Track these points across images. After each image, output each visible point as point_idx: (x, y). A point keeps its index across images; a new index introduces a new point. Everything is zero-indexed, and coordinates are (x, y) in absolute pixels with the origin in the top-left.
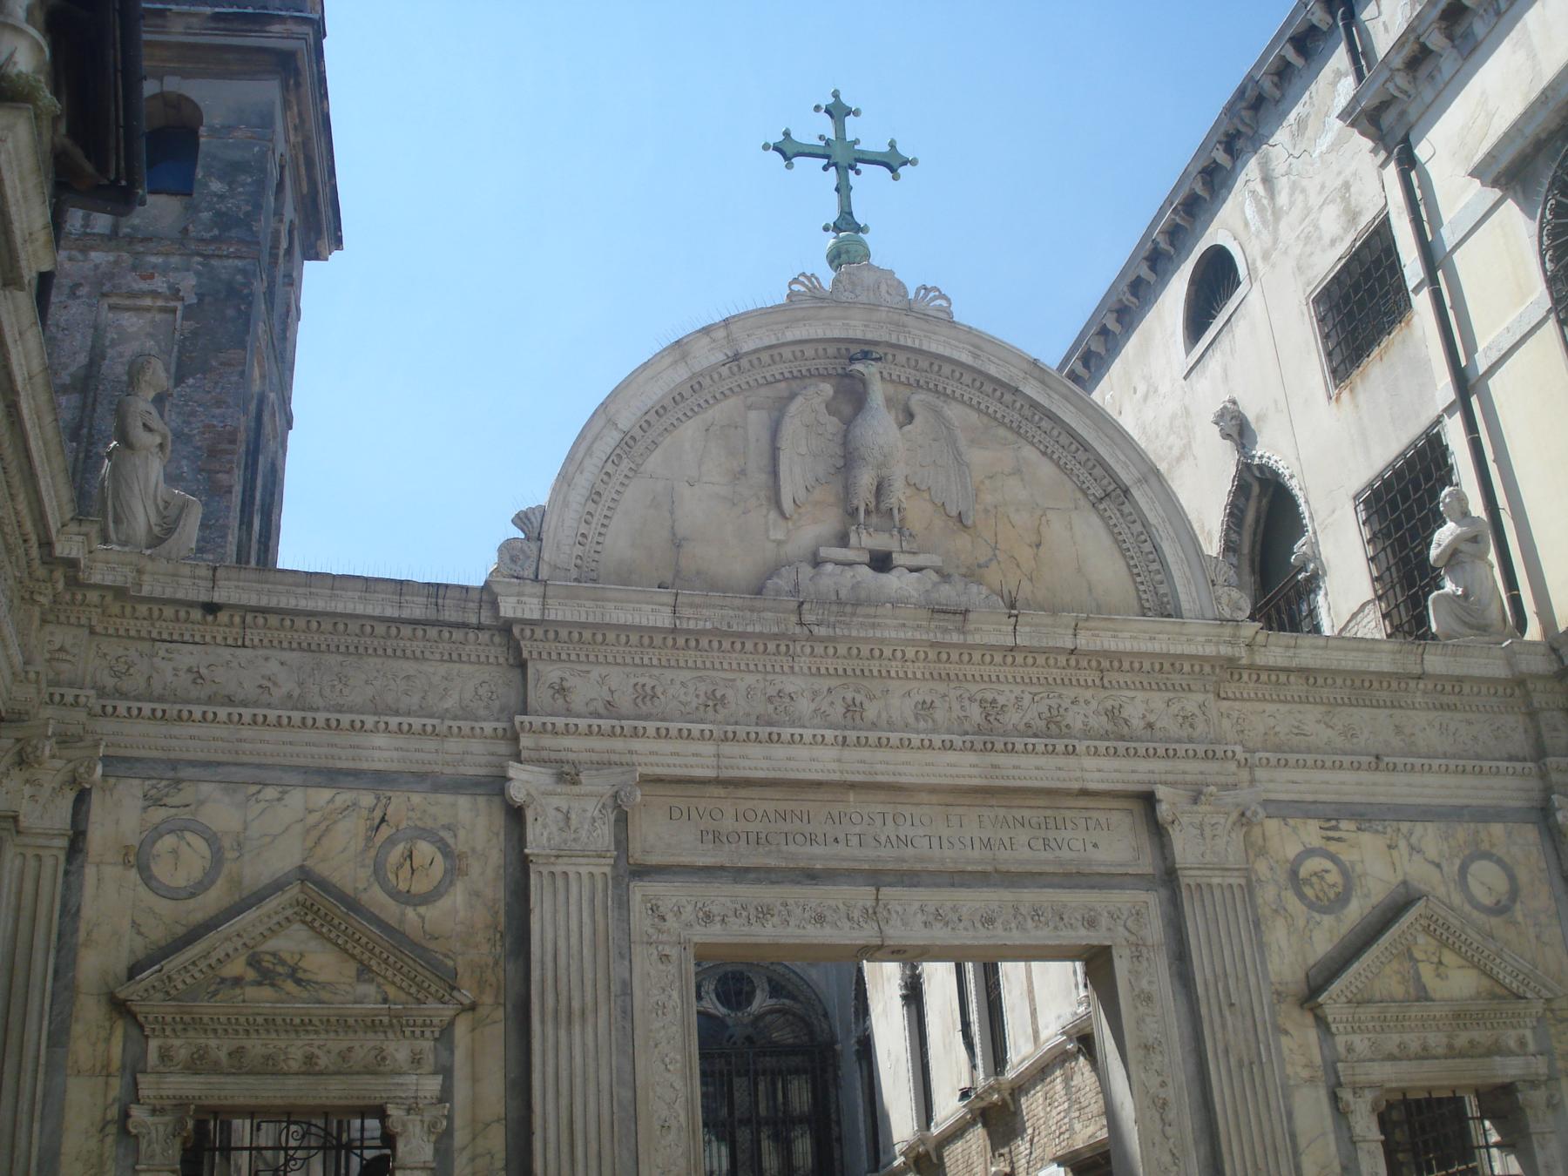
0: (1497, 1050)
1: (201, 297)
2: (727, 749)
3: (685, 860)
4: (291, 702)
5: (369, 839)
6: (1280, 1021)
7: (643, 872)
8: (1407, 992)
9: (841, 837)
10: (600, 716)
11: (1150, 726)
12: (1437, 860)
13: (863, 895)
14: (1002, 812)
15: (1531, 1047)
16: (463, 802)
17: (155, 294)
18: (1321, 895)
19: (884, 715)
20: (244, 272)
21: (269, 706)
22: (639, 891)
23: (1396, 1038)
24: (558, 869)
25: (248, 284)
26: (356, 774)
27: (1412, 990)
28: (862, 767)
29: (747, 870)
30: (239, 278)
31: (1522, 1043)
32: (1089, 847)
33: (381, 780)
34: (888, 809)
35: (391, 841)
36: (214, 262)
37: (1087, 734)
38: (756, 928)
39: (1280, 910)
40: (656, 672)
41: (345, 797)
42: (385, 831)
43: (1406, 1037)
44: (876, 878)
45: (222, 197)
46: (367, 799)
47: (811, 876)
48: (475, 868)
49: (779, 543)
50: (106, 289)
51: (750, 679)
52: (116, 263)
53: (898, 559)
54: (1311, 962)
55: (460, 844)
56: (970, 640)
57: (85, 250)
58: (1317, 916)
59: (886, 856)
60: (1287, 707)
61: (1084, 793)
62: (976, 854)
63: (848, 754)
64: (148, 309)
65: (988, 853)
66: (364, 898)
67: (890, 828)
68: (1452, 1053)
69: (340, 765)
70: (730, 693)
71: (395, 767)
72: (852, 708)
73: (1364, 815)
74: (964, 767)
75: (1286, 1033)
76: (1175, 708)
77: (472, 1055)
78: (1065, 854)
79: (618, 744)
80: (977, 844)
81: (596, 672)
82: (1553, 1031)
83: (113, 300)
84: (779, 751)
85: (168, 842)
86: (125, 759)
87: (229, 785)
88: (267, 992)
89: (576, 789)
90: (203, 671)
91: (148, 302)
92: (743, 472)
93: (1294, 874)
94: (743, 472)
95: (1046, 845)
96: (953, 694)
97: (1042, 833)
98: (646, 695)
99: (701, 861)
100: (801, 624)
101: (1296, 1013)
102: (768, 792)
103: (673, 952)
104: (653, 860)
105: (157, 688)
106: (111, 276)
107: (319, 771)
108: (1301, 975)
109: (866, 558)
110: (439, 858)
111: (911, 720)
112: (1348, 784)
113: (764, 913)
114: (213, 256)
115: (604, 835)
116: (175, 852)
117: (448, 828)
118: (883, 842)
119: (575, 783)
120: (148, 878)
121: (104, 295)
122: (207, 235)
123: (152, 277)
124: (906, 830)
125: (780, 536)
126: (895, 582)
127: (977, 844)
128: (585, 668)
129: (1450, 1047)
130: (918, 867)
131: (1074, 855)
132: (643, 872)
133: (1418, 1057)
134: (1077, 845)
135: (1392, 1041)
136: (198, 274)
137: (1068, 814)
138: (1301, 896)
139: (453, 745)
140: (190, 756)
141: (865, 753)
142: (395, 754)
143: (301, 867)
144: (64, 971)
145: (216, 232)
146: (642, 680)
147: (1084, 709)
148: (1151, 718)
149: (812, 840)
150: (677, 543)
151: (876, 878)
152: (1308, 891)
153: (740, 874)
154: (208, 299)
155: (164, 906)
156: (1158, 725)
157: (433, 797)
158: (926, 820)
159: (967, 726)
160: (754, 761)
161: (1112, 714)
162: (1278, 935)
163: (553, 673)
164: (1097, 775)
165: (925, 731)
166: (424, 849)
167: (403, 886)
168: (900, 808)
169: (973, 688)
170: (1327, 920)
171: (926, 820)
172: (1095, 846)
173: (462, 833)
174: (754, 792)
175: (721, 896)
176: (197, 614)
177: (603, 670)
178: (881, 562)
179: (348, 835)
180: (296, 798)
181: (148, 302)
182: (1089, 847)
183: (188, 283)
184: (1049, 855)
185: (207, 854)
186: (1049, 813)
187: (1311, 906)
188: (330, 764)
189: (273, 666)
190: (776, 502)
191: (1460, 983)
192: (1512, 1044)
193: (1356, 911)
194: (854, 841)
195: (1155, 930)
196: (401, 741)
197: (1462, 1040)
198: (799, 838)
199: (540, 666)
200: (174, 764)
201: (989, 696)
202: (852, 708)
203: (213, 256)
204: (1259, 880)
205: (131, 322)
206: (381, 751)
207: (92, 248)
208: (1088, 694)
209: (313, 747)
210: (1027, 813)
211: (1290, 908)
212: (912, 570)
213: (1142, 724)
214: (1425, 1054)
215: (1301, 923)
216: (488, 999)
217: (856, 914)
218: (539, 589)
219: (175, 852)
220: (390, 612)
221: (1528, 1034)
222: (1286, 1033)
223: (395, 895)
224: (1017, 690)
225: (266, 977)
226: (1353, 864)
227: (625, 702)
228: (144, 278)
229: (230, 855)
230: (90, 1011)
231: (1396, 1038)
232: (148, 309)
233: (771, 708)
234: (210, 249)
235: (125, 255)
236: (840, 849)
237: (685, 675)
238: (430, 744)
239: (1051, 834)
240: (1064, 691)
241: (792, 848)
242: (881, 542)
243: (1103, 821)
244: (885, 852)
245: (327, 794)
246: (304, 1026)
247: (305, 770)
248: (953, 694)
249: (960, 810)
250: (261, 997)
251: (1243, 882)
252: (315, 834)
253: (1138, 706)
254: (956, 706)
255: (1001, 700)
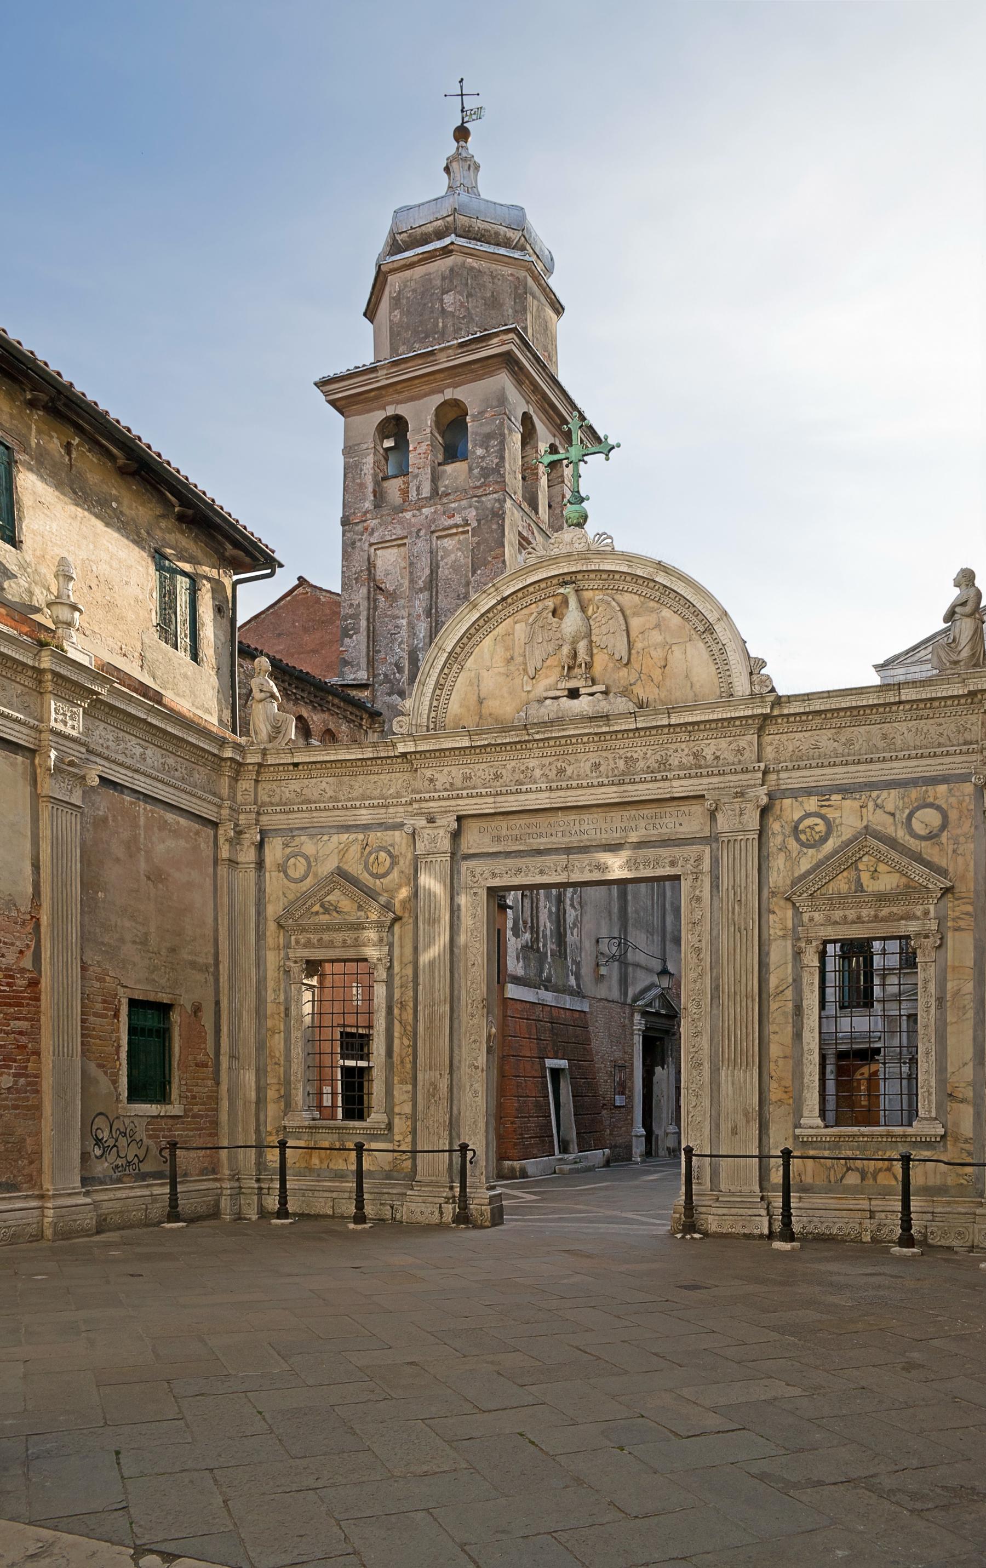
0: (908, 917)
1: (479, 521)
2: (499, 799)
3: (485, 850)
4: (335, 799)
5: (362, 853)
6: (771, 907)
7: (467, 857)
8: (850, 888)
9: (554, 833)
10: (448, 790)
11: (717, 758)
12: (893, 811)
13: (562, 859)
14: (633, 812)
15: (932, 914)
16: (397, 833)
17: (457, 526)
18: (810, 838)
19: (575, 772)
20: (498, 500)
21: (324, 802)
22: (464, 866)
23: (841, 913)
24: (429, 860)
25: (502, 507)
26: (357, 826)
27: (853, 888)
28: (560, 800)
29: (511, 852)
30: (497, 505)
31: (926, 913)
32: (677, 825)
33: (366, 828)
34: (577, 817)
35: (370, 853)
36: (483, 499)
37: (681, 767)
38: (514, 879)
39: (783, 848)
40: (471, 766)
41: (353, 836)
42: (368, 849)
43: (847, 912)
44: (568, 850)
45: (483, 458)
46: (361, 837)
47: (539, 852)
48: (401, 862)
49: (529, 692)
50: (432, 529)
51: (513, 763)
52: (435, 512)
53: (582, 691)
54: (796, 875)
55: (396, 853)
56: (612, 729)
57: (419, 509)
58: (805, 850)
59: (574, 840)
60: (810, 733)
61: (674, 799)
62: (618, 835)
63: (554, 794)
64: (456, 534)
65: (624, 834)
66: (360, 877)
67: (577, 828)
68: (876, 919)
69: (350, 823)
70: (504, 772)
71: (370, 822)
72: (561, 771)
73: (845, 790)
74: (611, 794)
75: (774, 913)
76: (733, 746)
77: (401, 938)
78: (664, 830)
79: (453, 803)
80: (619, 829)
81: (446, 769)
82: (950, 905)
83: (437, 534)
84: (522, 797)
85: (292, 860)
86: (275, 830)
87: (311, 836)
88: (327, 917)
89: (434, 825)
90: (299, 790)
91: (454, 531)
92: (512, 658)
93: (796, 828)
94: (512, 658)
95: (654, 827)
96: (610, 756)
97: (653, 821)
98: (467, 778)
99: (491, 850)
100: (528, 734)
101: (782, 903)
102: (521, 816)
103: (479, 891)
104: (472, 851)
105: (284, 800)
106: (434, 520)
107: (342, 826)
108: (789, 882)
109: (566, 693)
110: (388, 858)
111: (589, 773)
112: (840, 775)
113: (519, 870)
114: (482, 496)
115: (445, 844)
116: (295, 864)
117: (391, 845)
118: (573, 832)
119: (434, 822)
120: (287, 875)
121: (432, 532)
122: (478, 484)
123: (454, 516)
124: (585, 827)
125: (529, 688)
126: (583, 705)
127: (619, 829)
128: (441, 768)
129: (876, 916)
130: (588, 844)
131: (669, 830)
132: (467, 857)
133: (853, 922)
134: (670, 825)
135: (838, 915)
136: (477, 508)
137: (668, 809)
138: (798, 840)
139: (391, 810)
140: (297, 826)
141: (562, 793)
142: (369, 817)
143: (338, 868)
144: (260, 912)
145: (483, 480)
146: (465, 771)
147: (680, 753)
148: (718, 754)
149: (541, 836)
150: (481, 702)
151: (568, 850)
152: (803, 837)
153: (508, 854)
154: (483, 522)
155: (292, 886)
156: (722, 757)
157: (385, 833)
158: (595, 821)
159: (616, 772)
160: (511, 804)
161: (696, 755)
162: (778, 863)
163: (428, 773)
164: (680, 789)
165: (597, 777)
166: (383, 855)
167: (375, 871)
168: (582, 816)
169: (621, 752)
170: (811, 851)
171: (595, 821)
172: (681, 825)
173: (396, 847)
174: (515, 817)
175: (500, 865)
176: (291, 768)
177: (449, 768)
178: (574, 694)
179: (355, 850)
180: (335, 838)
181: (454, 531)
182: (677, 825)
183: (472, 514)
184: (655, 832)
185: (305, 864)
186: (658, 810)
187: (803, 845)
188: (346, 823)
189: (324, 784)
190: (525, 670)
191: (888, 882)
192: (919, 913)
193: (830, 846)
194: (560, 834)
195: (706, 866)
196: (371, 812)
197: (885, 912)
198: (535, 836)
199: (423, 770)
200: (291, 830)
201: (629, 755)
202: (561, 771)
203: (482, 496)
204: (773, 833)
205: (448, 543)
206: (364, 816)
207: (423, 507)
208: (683, 746)
209: (339, 817)
210: (646, 812)
211: (789, 847)
212: (592, 694)
213: (713, 757)
214: (859, 921)
215: (795, 854)
216: (407, 915)
217: (559, 869)
218: (411, 738)
219: (295, 864)
220: (360, 756)
221: (932, 908)
222: (774, 913)
223: (372, 875)
224: (644, 749)
225: (327, 911)
226: (834, 819)
227: (458, 783)
228: (449, 517)
229: (313, 864)
230: (272, 926)
231: (841, 913)
232: (456, 534)
233: (522, 776)
234: (480, 492)
235: (439, 506)
236: (553, 839)
237: (484, 766)
238: (383, 811)
239: (657, 821)
240: (669, 746)
241: (531, 840)
242: (572, 684)
243: (687, 812)
244: (574, 838)
245: (346, 836)
246: (339, 928)
247: (337, 827)
248: (610, 756)
249: (612, 814)
250: (324, 918)
251: (756, 836)
252: (342, 853)
253: (711, 747)
254: (612, 762)
255: (635, 756)
